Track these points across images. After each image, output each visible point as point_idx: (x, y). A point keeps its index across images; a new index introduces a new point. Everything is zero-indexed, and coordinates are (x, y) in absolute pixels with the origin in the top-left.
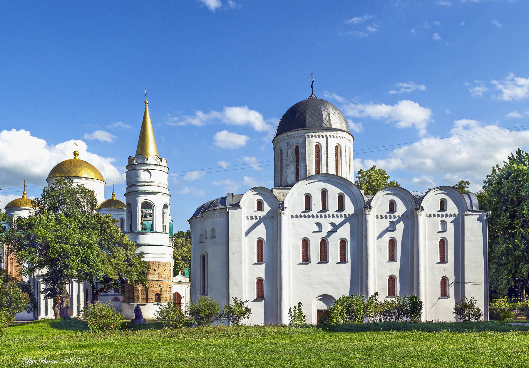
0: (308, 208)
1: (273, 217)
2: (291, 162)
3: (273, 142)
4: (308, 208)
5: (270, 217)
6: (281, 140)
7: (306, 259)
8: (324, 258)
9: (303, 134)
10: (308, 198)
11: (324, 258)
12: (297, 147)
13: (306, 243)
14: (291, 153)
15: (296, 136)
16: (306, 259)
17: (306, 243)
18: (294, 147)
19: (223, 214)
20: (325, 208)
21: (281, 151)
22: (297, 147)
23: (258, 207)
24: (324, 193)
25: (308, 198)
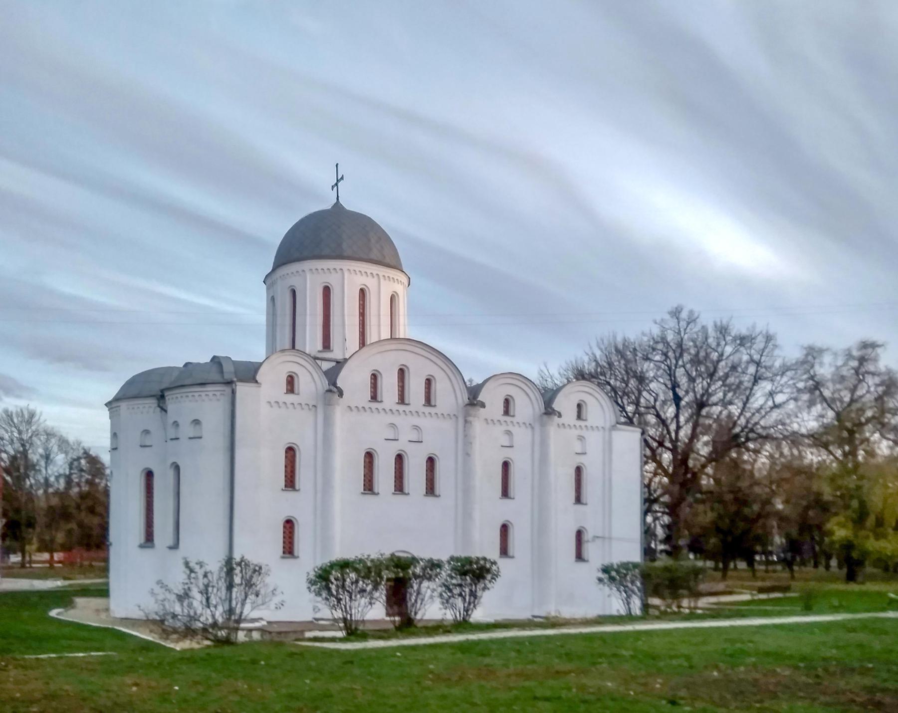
1: (314, 406)
3: (267, 276)
5: (311, 407)
7: (369, 486)
8: (399, 487)
11: (399, 487)
13: (369, 457)
16: (369, 486)
17: (369, 457)
19: (221, 394)
21: (294, 293)
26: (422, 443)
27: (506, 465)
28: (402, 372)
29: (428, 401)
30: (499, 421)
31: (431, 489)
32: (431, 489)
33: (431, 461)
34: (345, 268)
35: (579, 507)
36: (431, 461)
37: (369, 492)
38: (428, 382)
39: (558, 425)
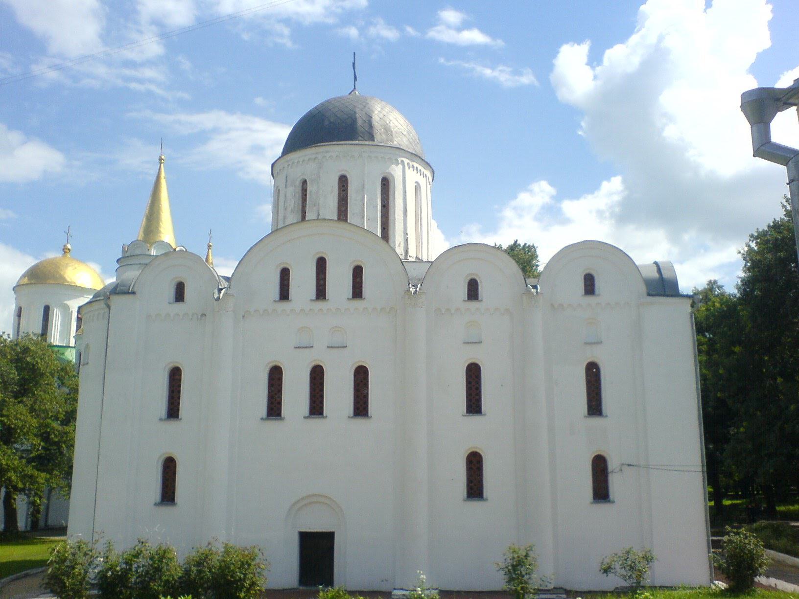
0: (284, 295)
2: (292, 211)
4: (284, 295)
6: (279, 171)
7: (274, 409)
8: (316, 407)
9: (314, 156)
10: (285, 274)
11: (316, 407)
12: (305, 182)
14: (292, 193)
15: (301, 160)
16: (274, 409)
18: (298, 183)
20: (321, 293)
22: (305, 182)
23: (178, 296)
24: (321, 264)
25: (285, 274)
26: (346, 349)
27: (473, 373)
28: (321, 264)
29: (357, 292)
30: (458, 309)
31: (361, 408)
32: (361, 408)
33: (361, 375)
34: (320, 156)
35: (596, 421)
36: (361, 375)
37: (279, 418)
38: (358, 272)
39: (552, 305)
